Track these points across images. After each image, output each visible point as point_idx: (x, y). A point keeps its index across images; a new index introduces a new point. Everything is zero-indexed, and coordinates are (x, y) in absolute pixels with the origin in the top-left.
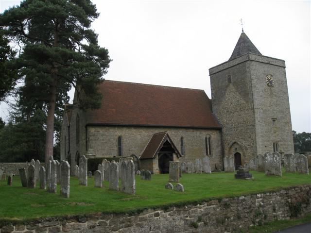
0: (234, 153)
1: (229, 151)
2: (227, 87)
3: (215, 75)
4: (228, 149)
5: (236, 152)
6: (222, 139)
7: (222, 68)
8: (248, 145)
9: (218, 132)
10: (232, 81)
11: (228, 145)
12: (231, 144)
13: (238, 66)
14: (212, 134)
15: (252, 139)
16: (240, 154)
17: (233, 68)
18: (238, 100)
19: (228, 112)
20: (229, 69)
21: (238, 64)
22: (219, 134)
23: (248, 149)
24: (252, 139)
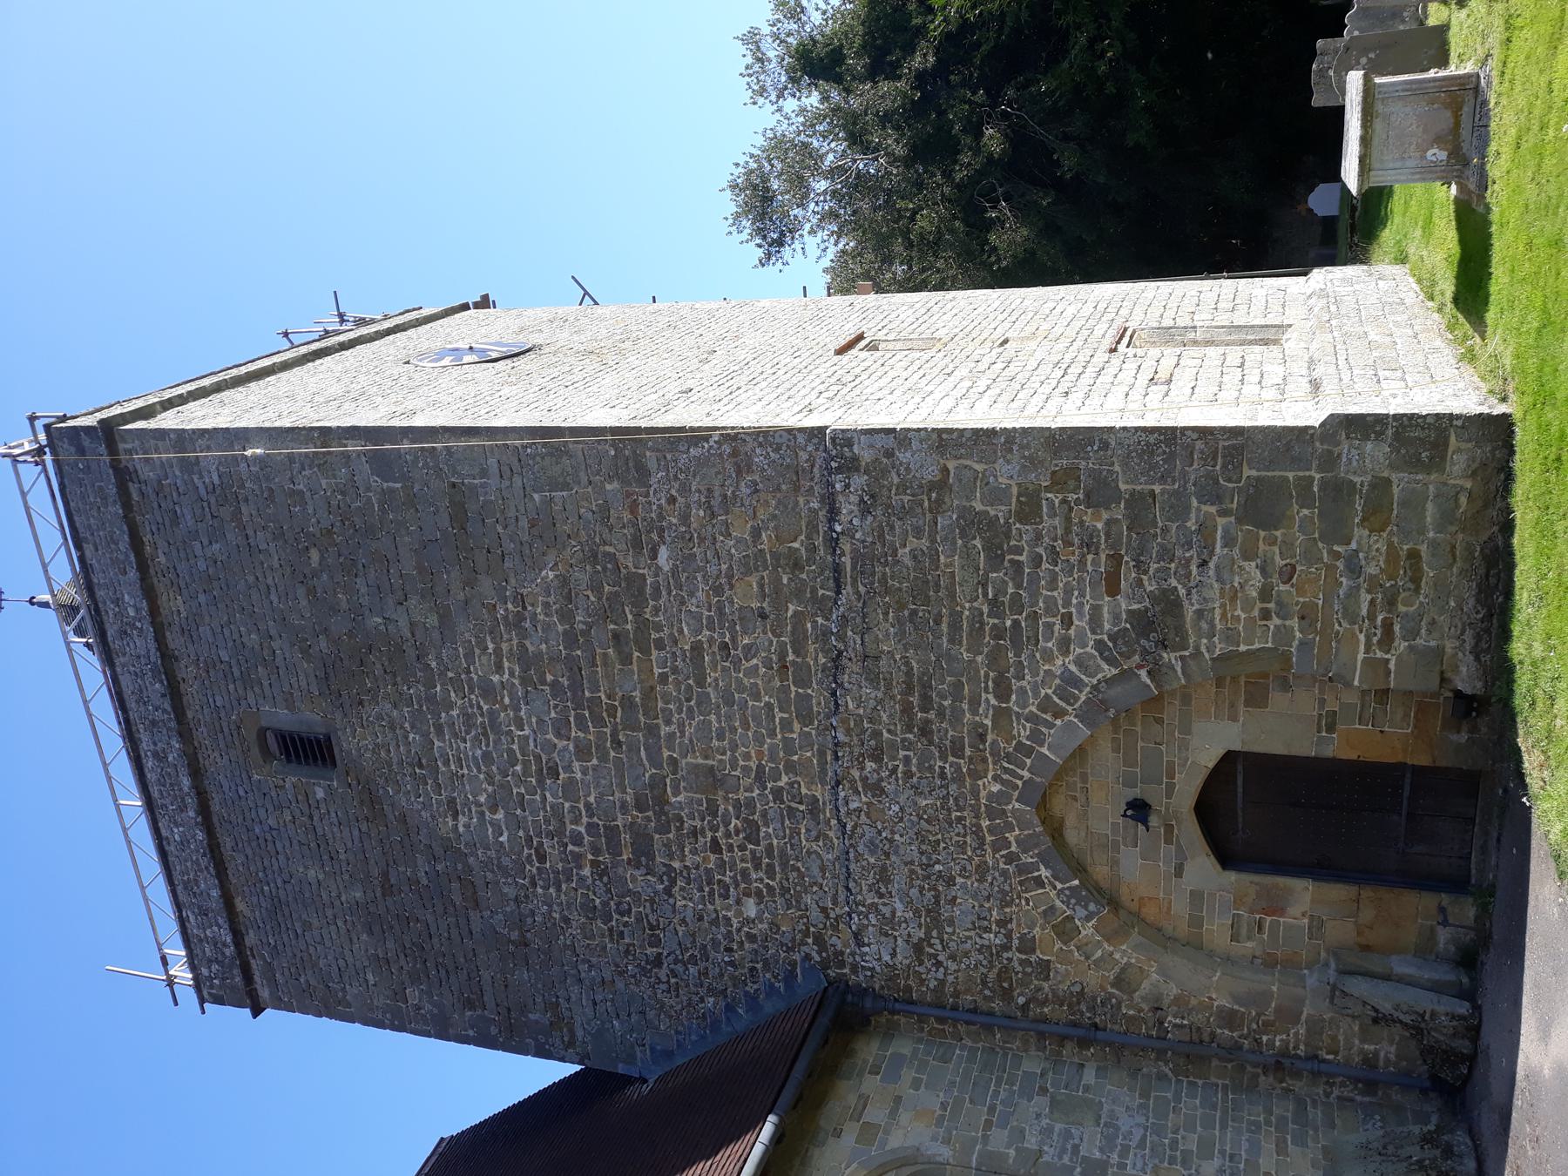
0: (1202, 867)
1: (1160, 938)
2: (372, 799)
3: (251, 939)
4: (1124, 954)
5: (1191, 830)
6: (979, 1020)
7: (185, 829)
8: (1113, 590)
9: (869, 1050)
10: (308, 717)
11: (1065, 931)
12: (1053, 893)
13: (174, 604)
14: (869, 1133)
15: (1029, 509)
16: (1229, 758)
17: (186, 671)
18: (523, 658)
19: (643, 852)
20: (202, 735)
21: (149, 593)
22: (903, 1046)
23: (1169, 603)
24: (1029, 509)
